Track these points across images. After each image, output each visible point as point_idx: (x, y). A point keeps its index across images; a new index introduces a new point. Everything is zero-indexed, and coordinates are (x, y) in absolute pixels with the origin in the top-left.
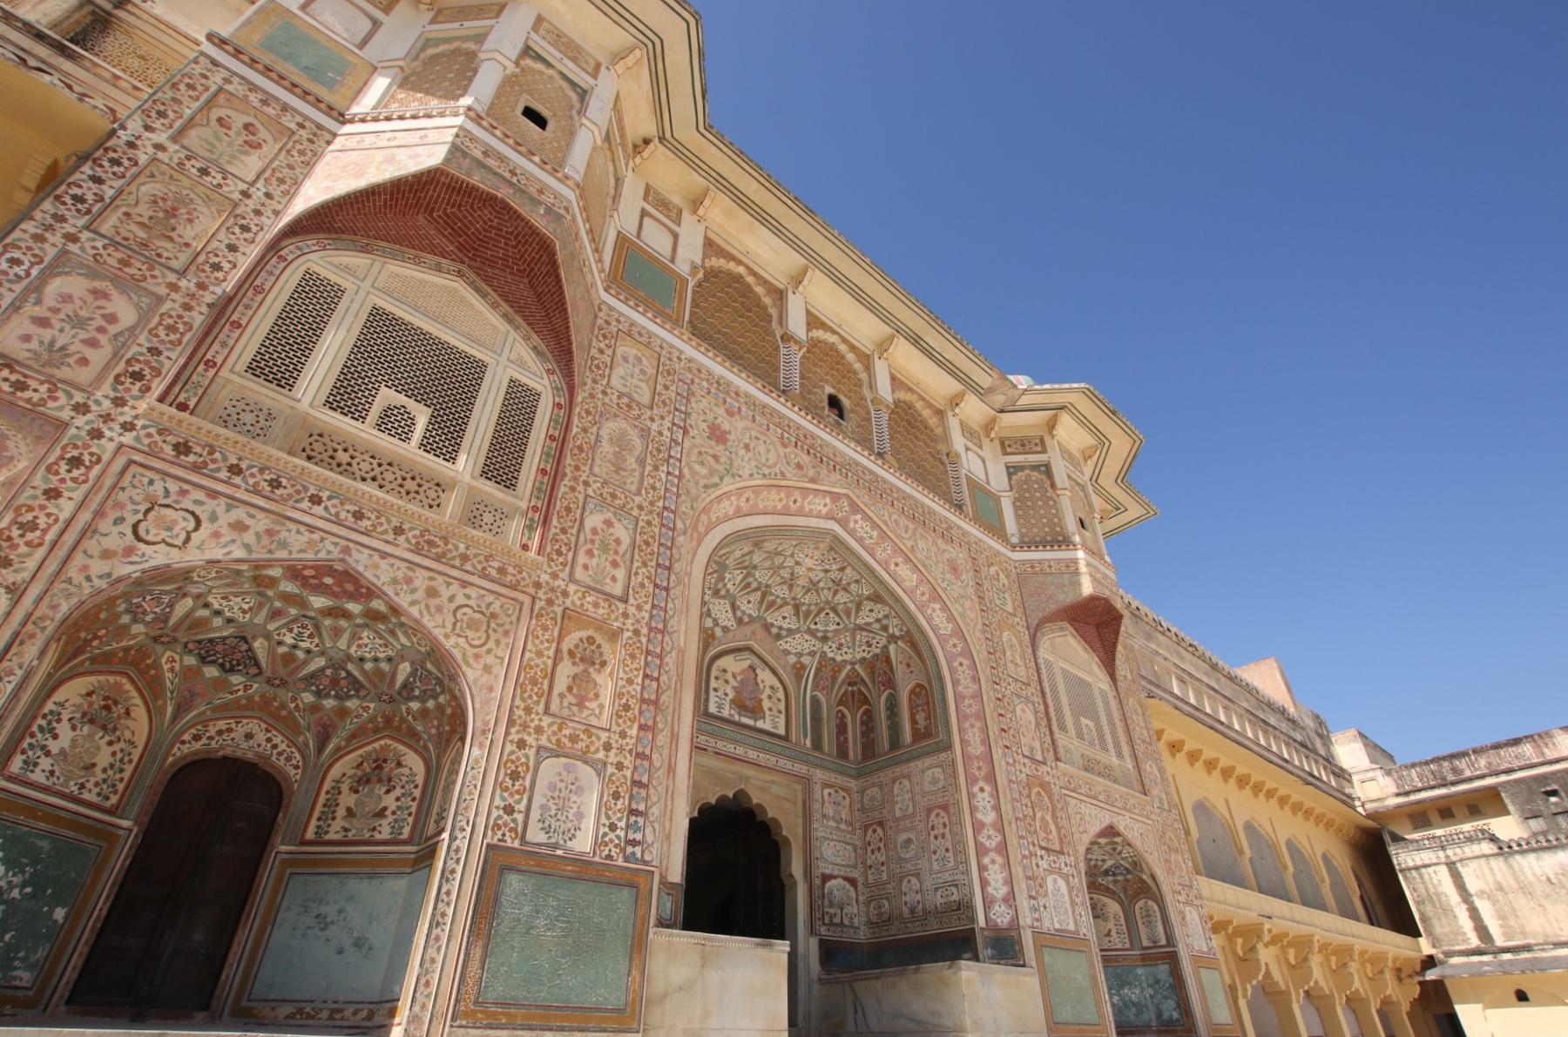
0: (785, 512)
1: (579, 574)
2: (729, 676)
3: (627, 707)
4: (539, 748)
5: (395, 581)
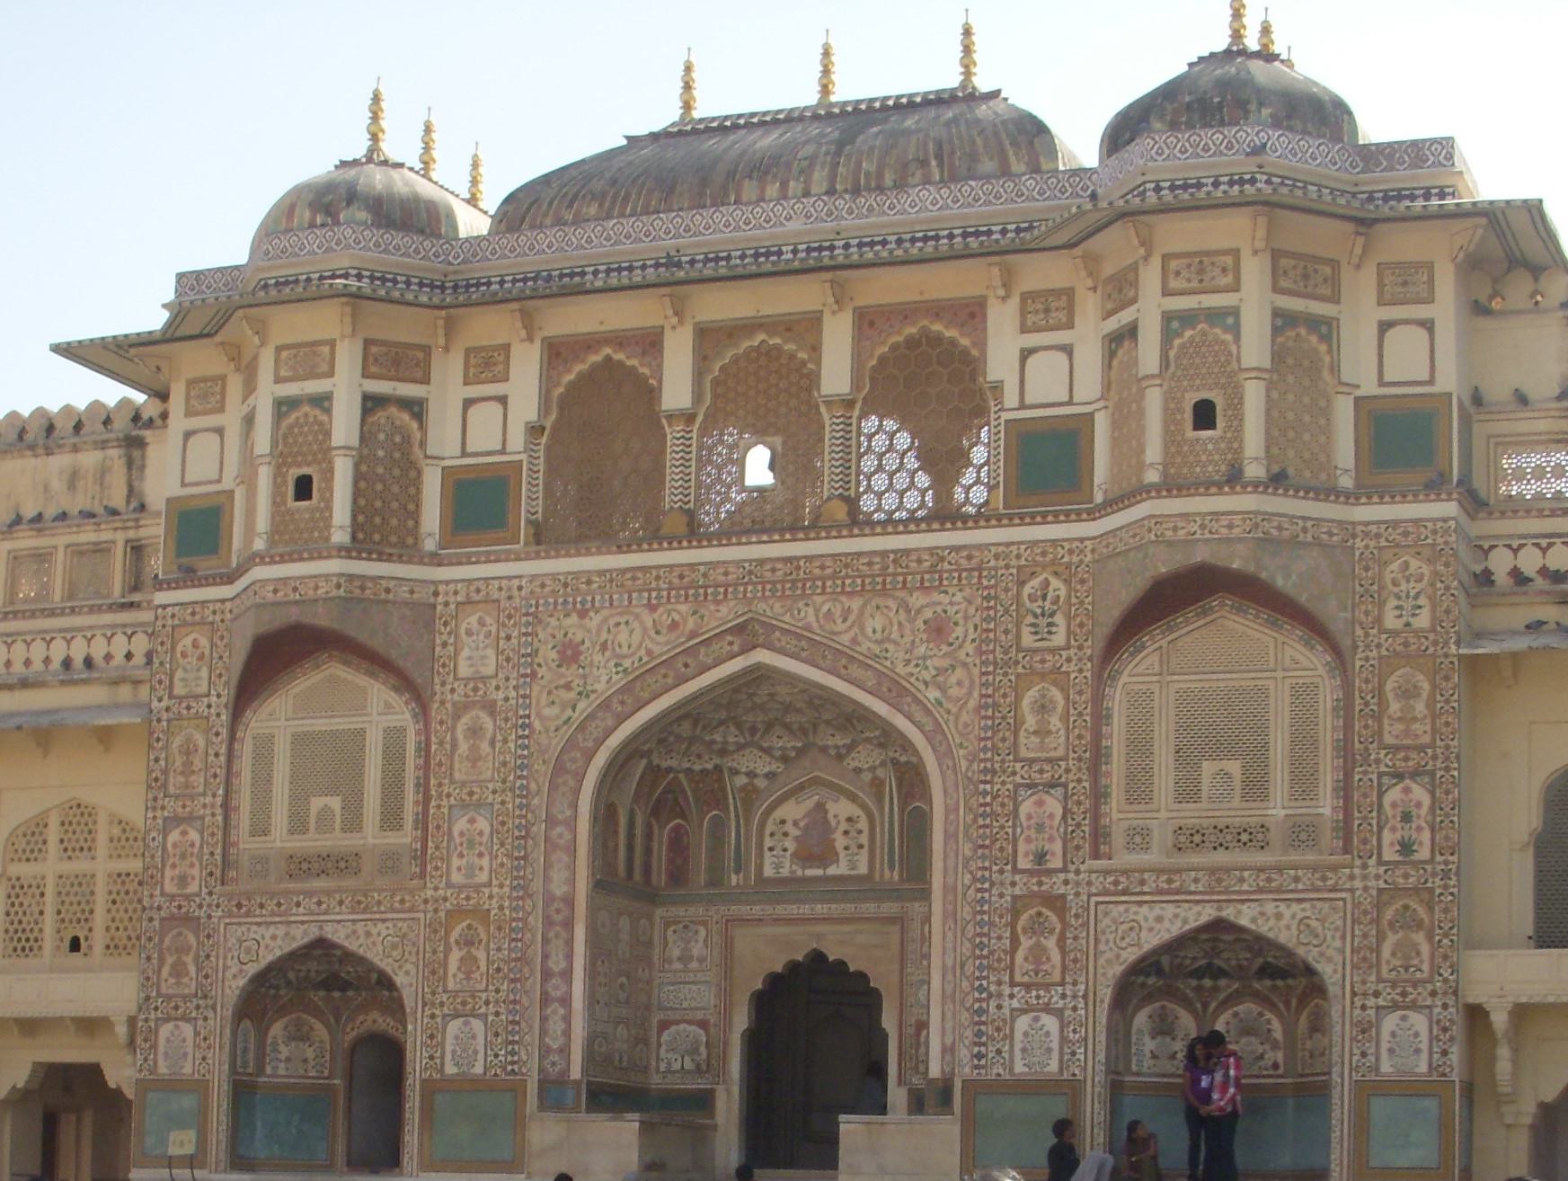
1: (456, 878)
2: (789, 828)
3: (498, 970)
4: (444, 1016)
5: (348, 937)
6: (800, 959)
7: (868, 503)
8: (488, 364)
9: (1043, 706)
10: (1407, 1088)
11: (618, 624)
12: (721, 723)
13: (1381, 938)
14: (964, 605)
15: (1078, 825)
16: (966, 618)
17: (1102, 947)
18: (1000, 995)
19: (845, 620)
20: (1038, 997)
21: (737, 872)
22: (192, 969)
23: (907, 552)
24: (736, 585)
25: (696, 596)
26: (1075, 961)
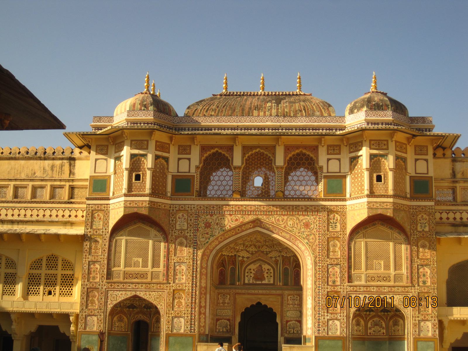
0: (236, 234)
2: (252, 271)
3: (188, 305)
5: (144, 295)
6: (255, 304)
7: (287, 193)
8: (184, 150)
9: (334, 245)
10: (427, 340)
11: (221, 219)
12: (241, 244)
14: (313, 220)
15: (344, 274)
16: (314, 223)
18: (324, 315)
19: (282, 222)
20: (334, 316)
21: (239, 281)
22: (97, 302)
23: (299, 206)
24: (253, 211)
25: (243, 213)
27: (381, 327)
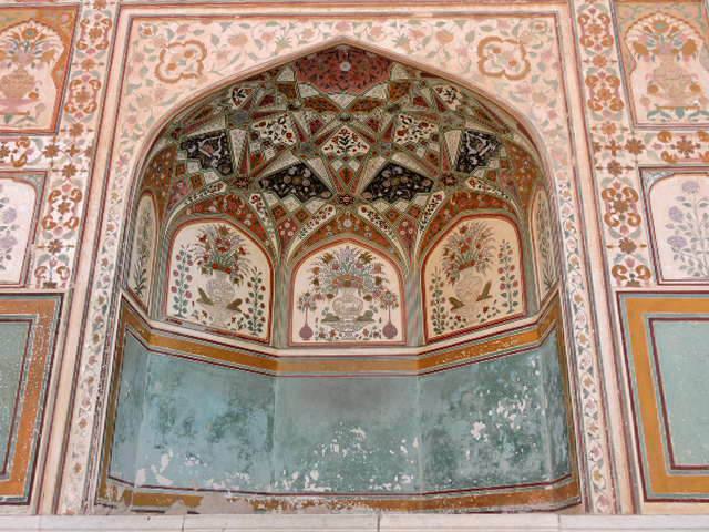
13: (627, 67)
17: (132, 80)
26: (83, 97)
27: (377, 290)
